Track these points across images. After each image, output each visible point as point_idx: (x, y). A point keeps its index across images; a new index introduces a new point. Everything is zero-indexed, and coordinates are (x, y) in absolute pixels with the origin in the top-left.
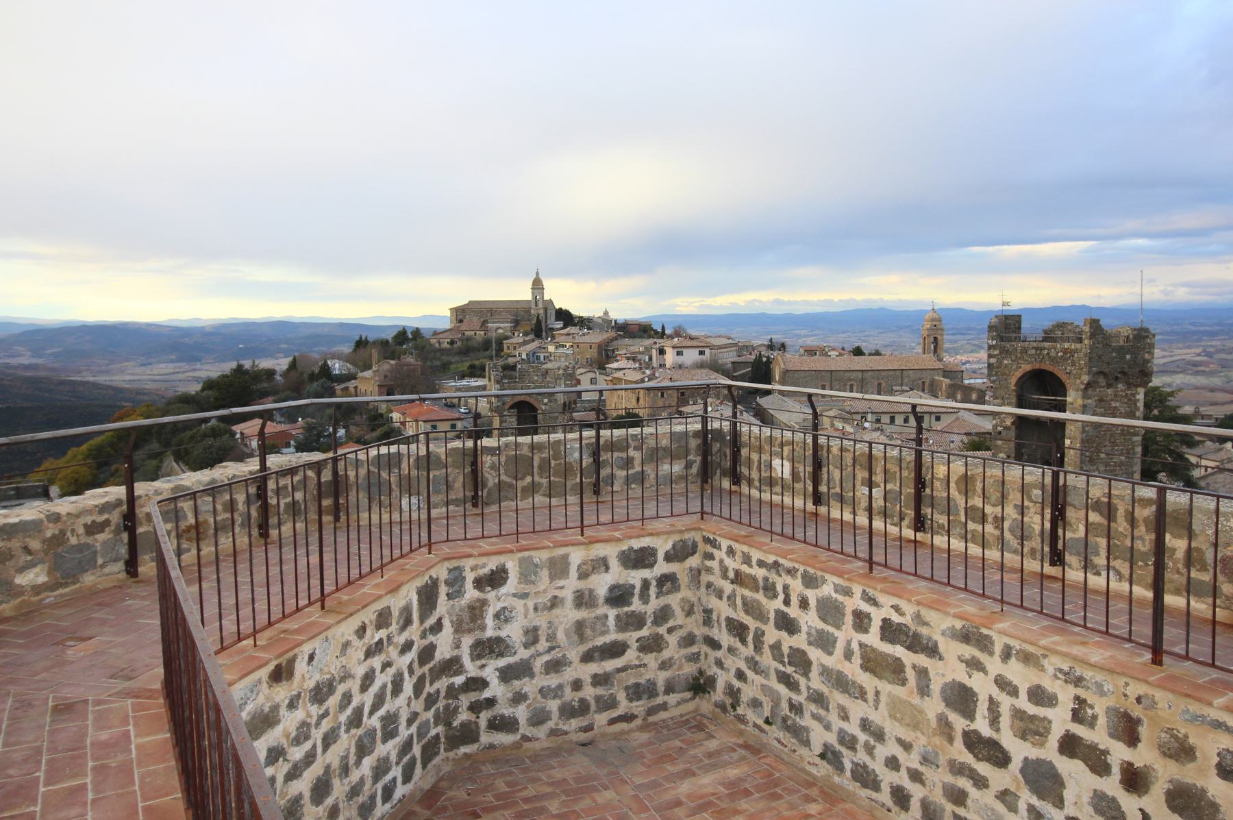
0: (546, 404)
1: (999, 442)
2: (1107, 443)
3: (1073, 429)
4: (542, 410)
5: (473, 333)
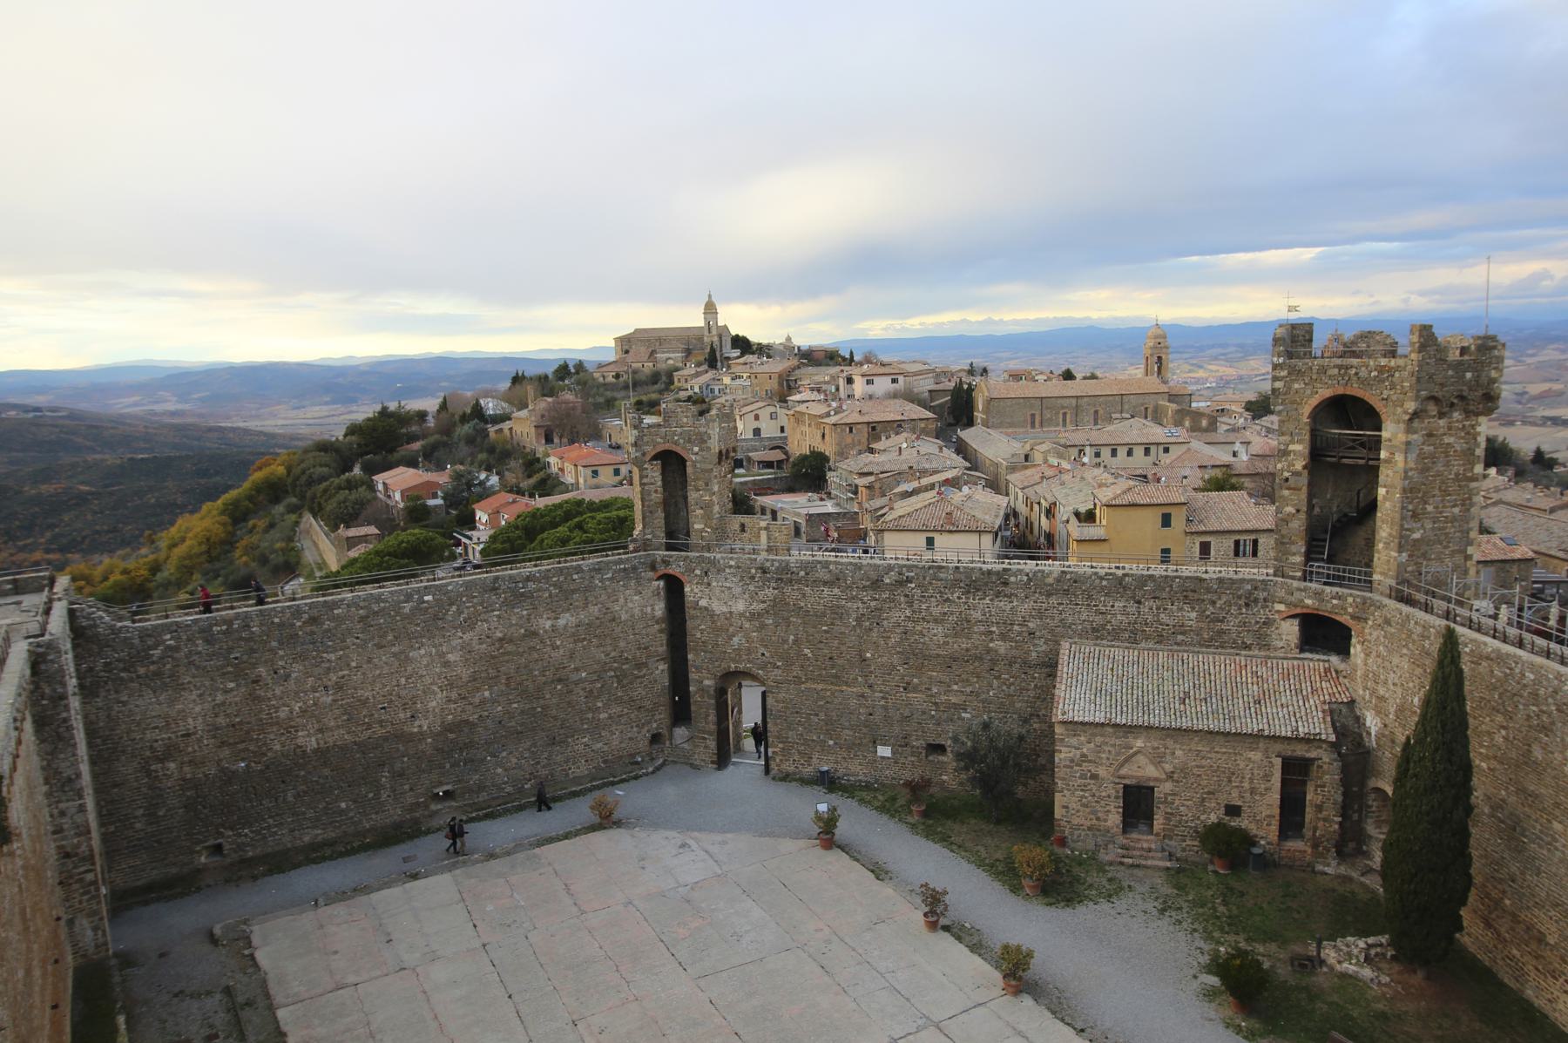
1: (1286, 493)
2: (1437, 492)
3: (1391, 474)
4: (692, 461)
5: (640, 365)
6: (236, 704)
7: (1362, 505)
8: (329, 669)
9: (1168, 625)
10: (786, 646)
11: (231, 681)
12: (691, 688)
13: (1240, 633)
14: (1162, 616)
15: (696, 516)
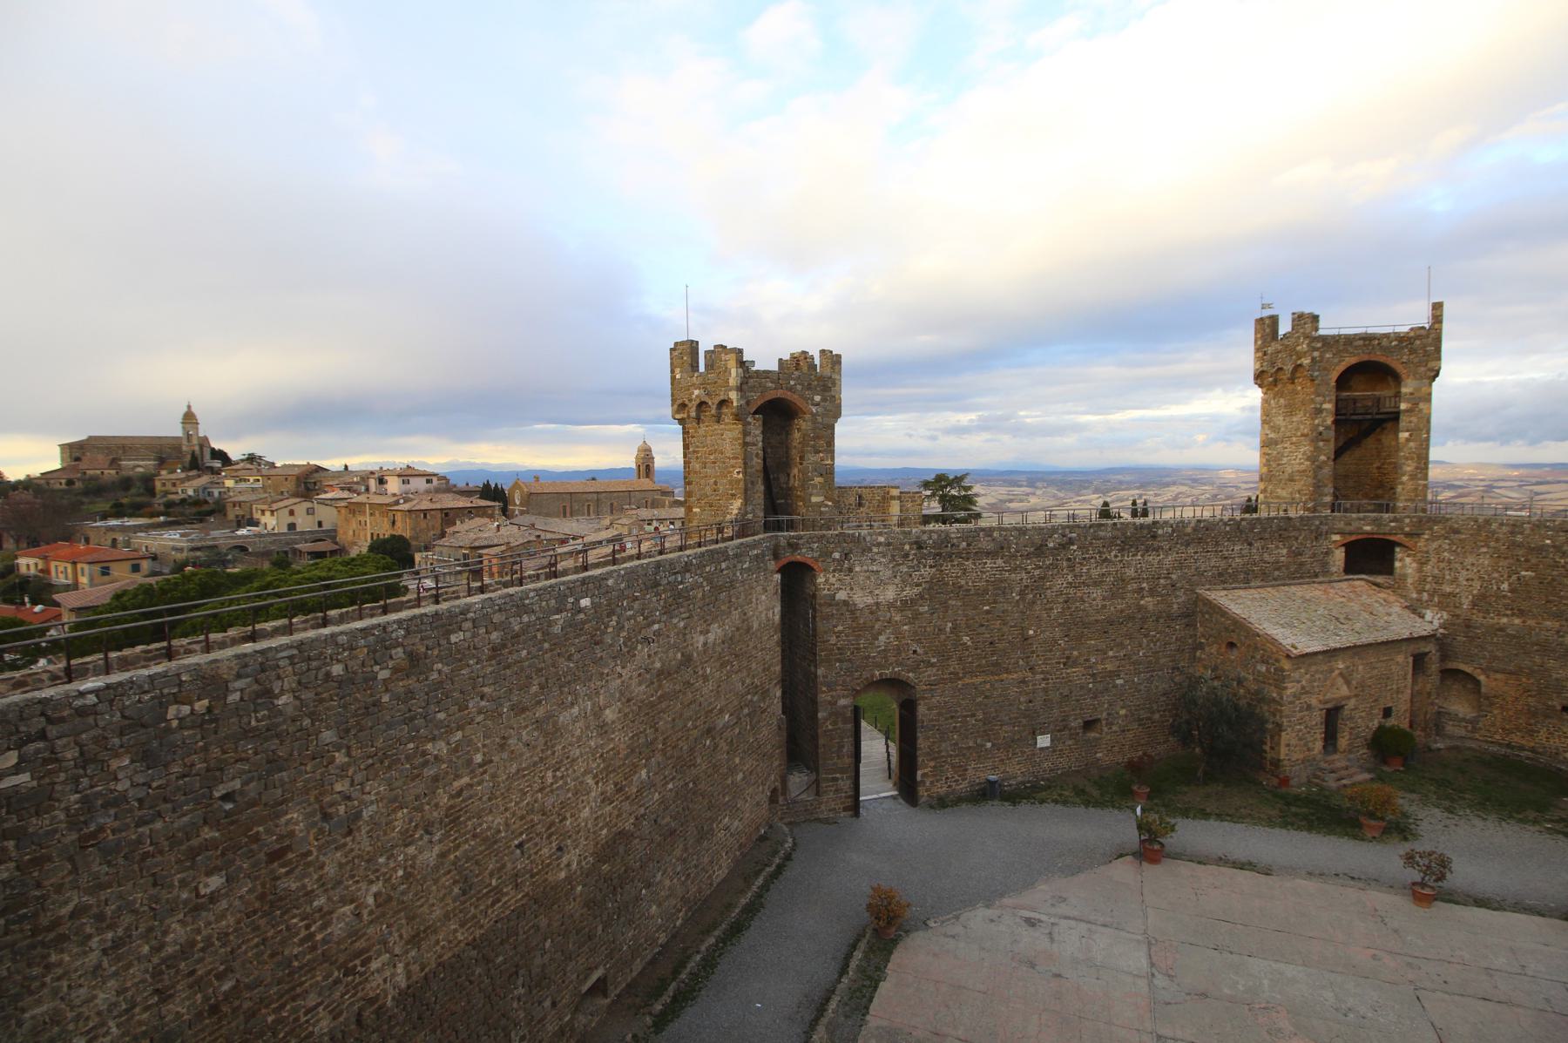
0: (818, 404)
4: (812, 413)
5: (99, 472)
6: (224, 936)
8: (436, 779)
10: (943, 637)
11: (209, 874)
12: (820, 715)
15: (814, 486)
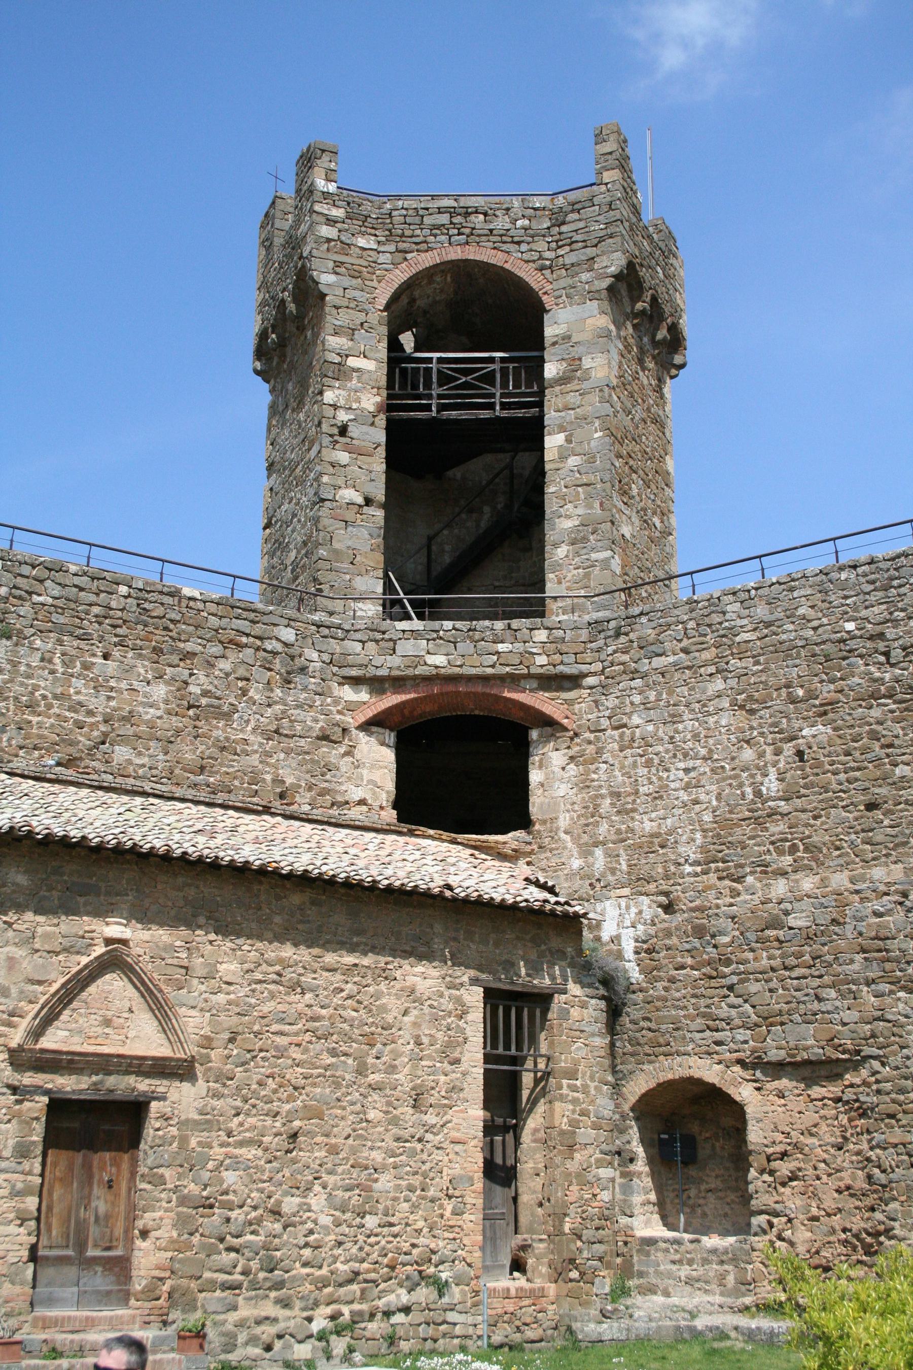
7: (434, 574)
9: (90, 713)
13: (269, 755)
14: (78, 683)
